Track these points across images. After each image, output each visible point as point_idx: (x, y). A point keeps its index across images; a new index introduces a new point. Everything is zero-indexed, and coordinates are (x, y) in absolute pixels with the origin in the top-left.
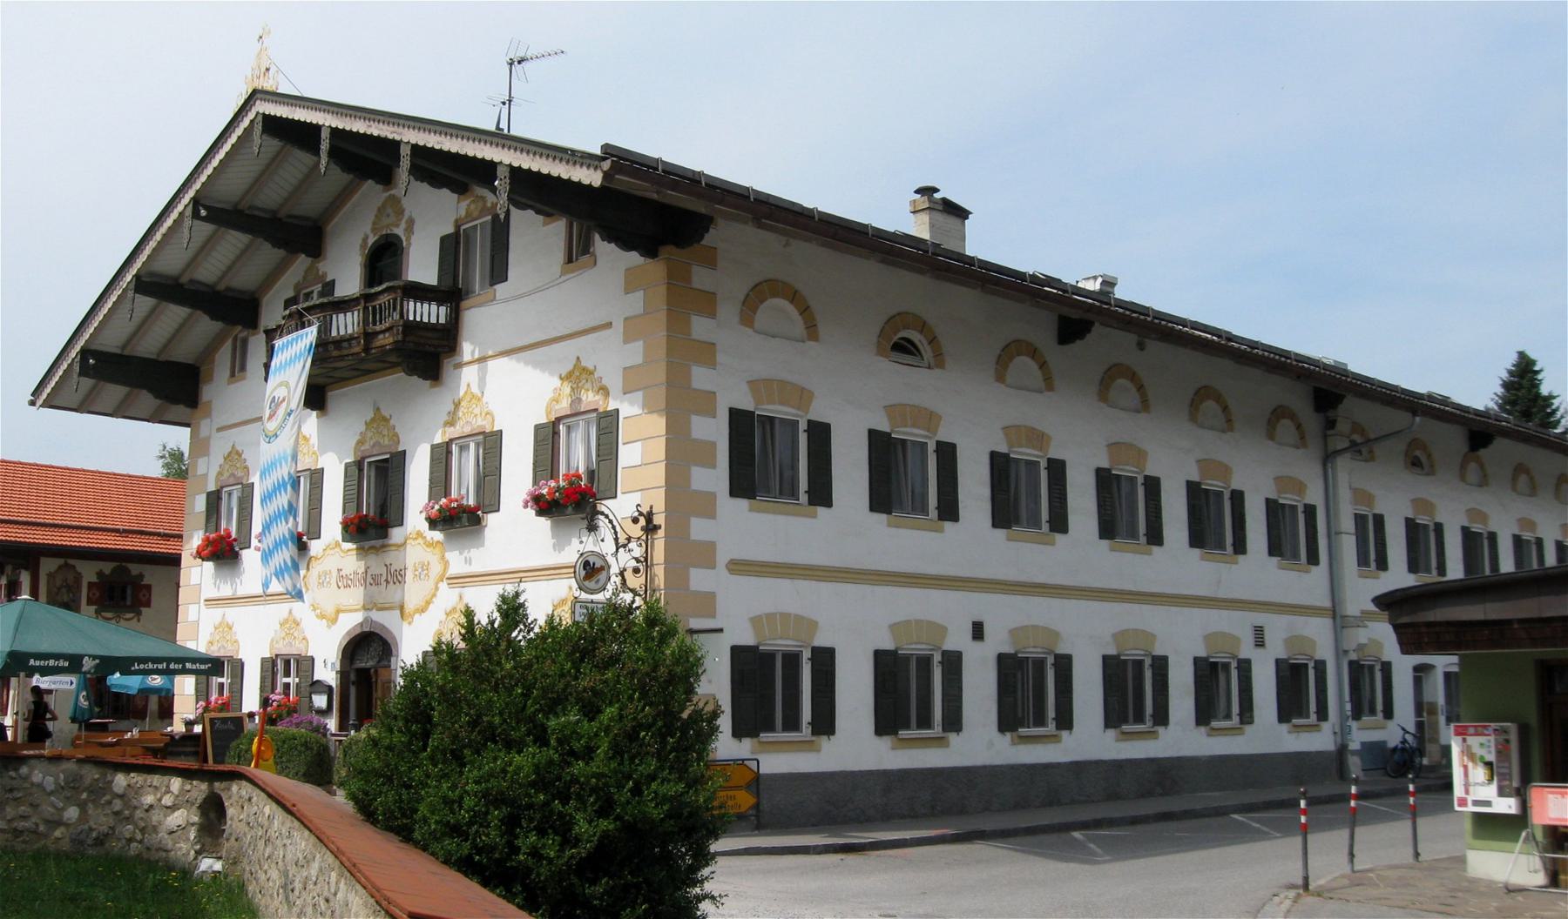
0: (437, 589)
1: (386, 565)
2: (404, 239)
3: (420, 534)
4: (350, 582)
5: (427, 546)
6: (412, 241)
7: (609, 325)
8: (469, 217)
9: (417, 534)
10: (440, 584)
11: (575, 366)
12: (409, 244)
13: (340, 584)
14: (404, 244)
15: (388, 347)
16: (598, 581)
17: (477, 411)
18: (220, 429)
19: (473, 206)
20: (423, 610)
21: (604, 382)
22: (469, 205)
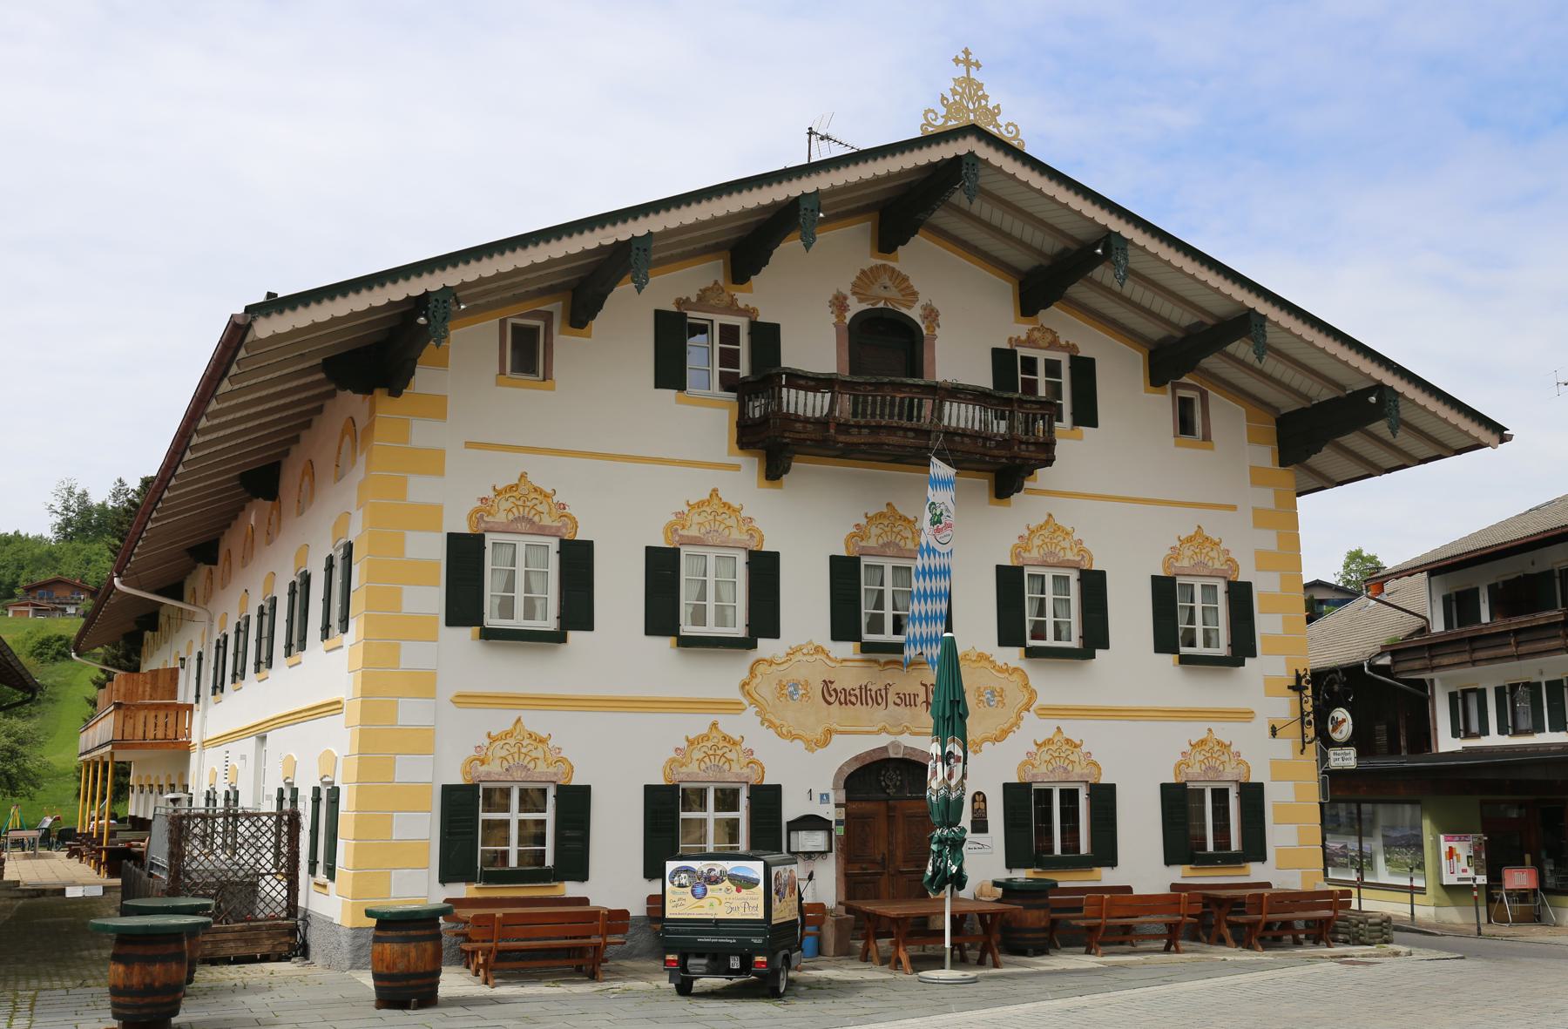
0: (1019, 717)
1: (925, 686)
2: (923, 327)
3: (982, 657)
4: (853, 699)
5: (999, 671)
6: (938, 332)
7: (1233, 508)
8: (1030, 342)
9: (978, 656)
10: (1025, 714)
11: (1196, 532)
12: (934, 337)
13: (831, 700)
14: (925, 332)
15: (1033, 462)
16: (1341, 733)
17: (1066, 544)
18: (469, 445)
19: (1037, 334)
20: (997, 739)
21: (1232, 555)
22: (1033, 330)
